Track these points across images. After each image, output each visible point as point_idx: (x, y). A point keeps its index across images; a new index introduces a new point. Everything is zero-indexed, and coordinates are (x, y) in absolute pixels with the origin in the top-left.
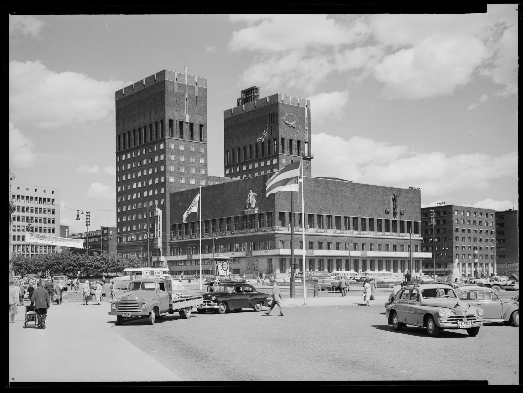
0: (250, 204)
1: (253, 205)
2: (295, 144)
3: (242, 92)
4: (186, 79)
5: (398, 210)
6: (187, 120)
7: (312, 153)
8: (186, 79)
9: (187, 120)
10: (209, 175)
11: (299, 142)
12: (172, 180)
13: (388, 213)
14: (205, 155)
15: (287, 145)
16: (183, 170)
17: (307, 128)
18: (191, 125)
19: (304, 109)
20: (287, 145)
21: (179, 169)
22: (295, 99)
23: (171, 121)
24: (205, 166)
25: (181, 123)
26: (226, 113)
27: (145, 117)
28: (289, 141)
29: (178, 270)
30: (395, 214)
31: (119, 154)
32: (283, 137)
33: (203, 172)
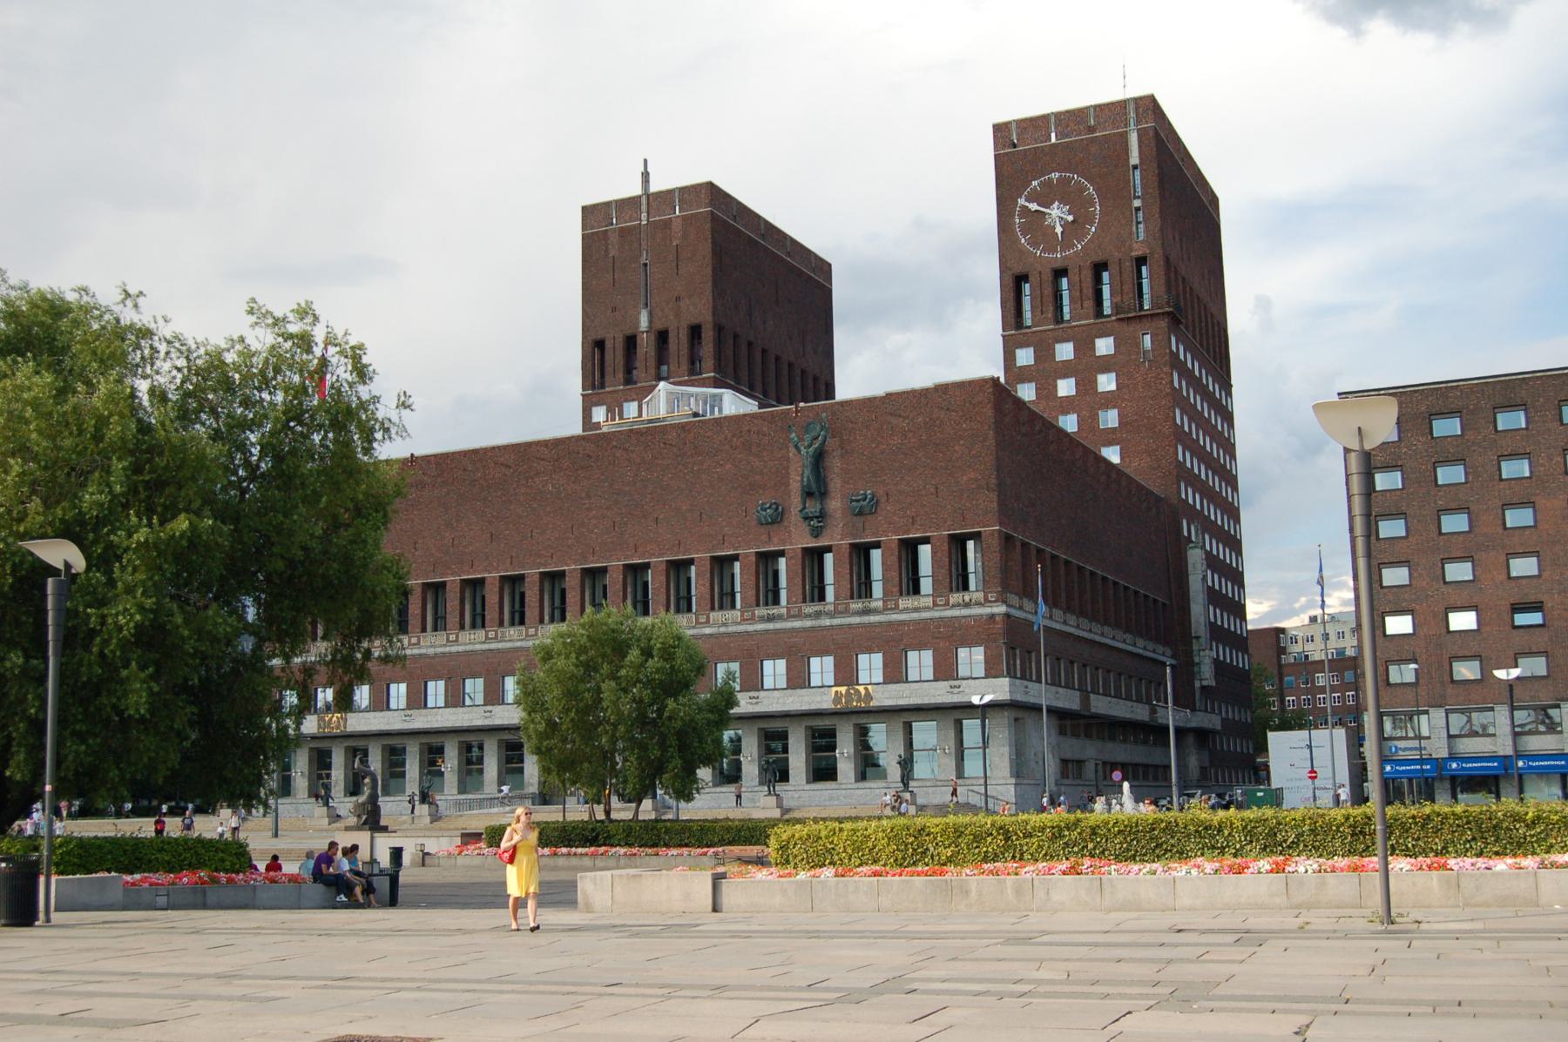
4: (644, 207)
5: (835, 504)
8: (644, 207)
17: (1137, 203)
18: (662, 337)
19: (1124, 137)
25: (631, 342)
28: (1048, 277)
30: (818, 522)
32: (1019, 269)
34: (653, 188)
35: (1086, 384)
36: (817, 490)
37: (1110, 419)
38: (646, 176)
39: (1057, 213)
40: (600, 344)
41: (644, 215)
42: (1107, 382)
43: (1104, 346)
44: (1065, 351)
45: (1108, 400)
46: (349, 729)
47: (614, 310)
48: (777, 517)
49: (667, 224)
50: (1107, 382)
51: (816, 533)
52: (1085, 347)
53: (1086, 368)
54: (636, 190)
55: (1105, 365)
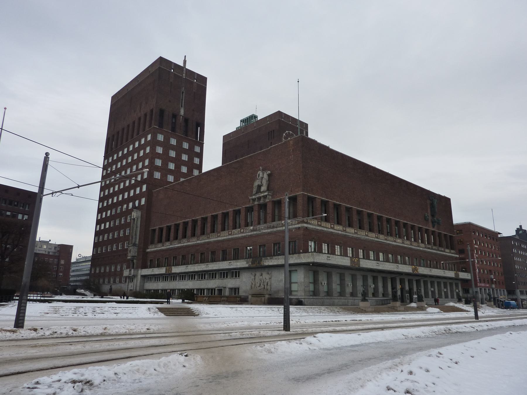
0: (259, 187)
1: (263, 188)
3: (241, 121)
4: (184, 72)
8: (184, 72)
9: (182, 112)
12: (157, 175)
13: (426, 220)
14: (200, 155)
16: (172, 166)
18: (186, 120)
21: (167, 165)
23: (162, 112)
24: (199, 167)
25: (175, 116)
26: (225, 137)
27: (135, 112)
29: (154, 288)
34: (188, 67)
38: (185, 62)
41: (184, 75)
46: (361, 266)
47: (170, 101)
49: (192, 83)
51: (433, 227)
54: (182, 64)
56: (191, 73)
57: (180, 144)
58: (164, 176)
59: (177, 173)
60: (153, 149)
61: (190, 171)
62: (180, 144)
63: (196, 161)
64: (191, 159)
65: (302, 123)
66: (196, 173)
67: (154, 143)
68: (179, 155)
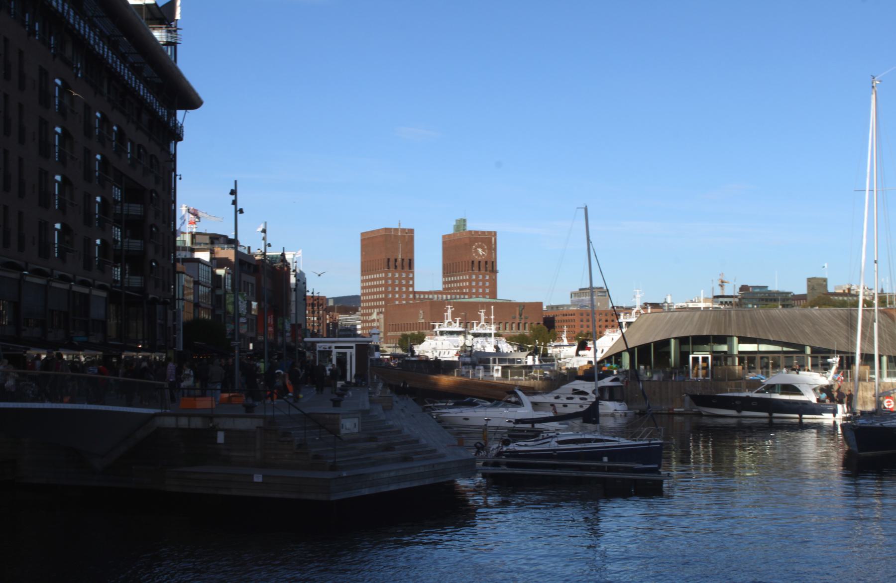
2: (483, 264)
6: (400, 257)
7: (498, 268)
10: (416, 290)
11: (486, 262)
14: (413, 279)
15: (476, 264)
18: (403, 260)
20: (476, 264)
22: (483, 233)
24: (413, 286)
31: (362, 275)
33: (411, 289)
35: (484, 284)
36: (520, 315)
37: (487, 291)
39: (480, 250)
40: (389, 259)
42: (487, 284)
43: (487, 277)
44: (481, 277)
45: (487, 287)
48: (515, 318)
50: (487, 284)
52: (484, 277)
53: (484, 281)
54: (397, 227)
55: (487, 280)
56: (403, 230)
57: (400, 275)
58: (393, 295)
59: (400, 292)
60: (386, 282)
61: (407, 289)
62: (400, 275)
63: (411, 282)
64: (408, 282)
65: (490, 233)
66: (411, 289)
67: (386, 279)
68: (400, 282)
